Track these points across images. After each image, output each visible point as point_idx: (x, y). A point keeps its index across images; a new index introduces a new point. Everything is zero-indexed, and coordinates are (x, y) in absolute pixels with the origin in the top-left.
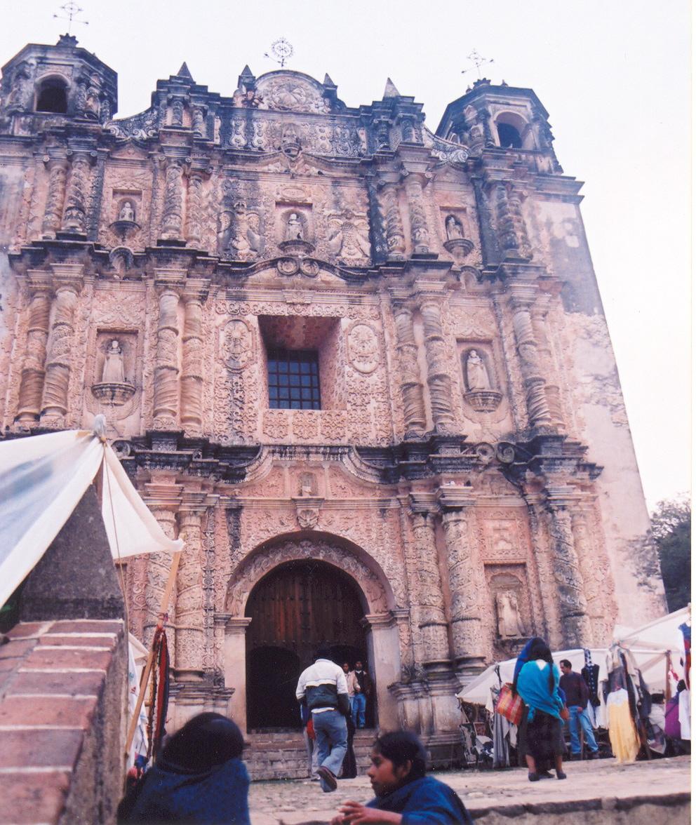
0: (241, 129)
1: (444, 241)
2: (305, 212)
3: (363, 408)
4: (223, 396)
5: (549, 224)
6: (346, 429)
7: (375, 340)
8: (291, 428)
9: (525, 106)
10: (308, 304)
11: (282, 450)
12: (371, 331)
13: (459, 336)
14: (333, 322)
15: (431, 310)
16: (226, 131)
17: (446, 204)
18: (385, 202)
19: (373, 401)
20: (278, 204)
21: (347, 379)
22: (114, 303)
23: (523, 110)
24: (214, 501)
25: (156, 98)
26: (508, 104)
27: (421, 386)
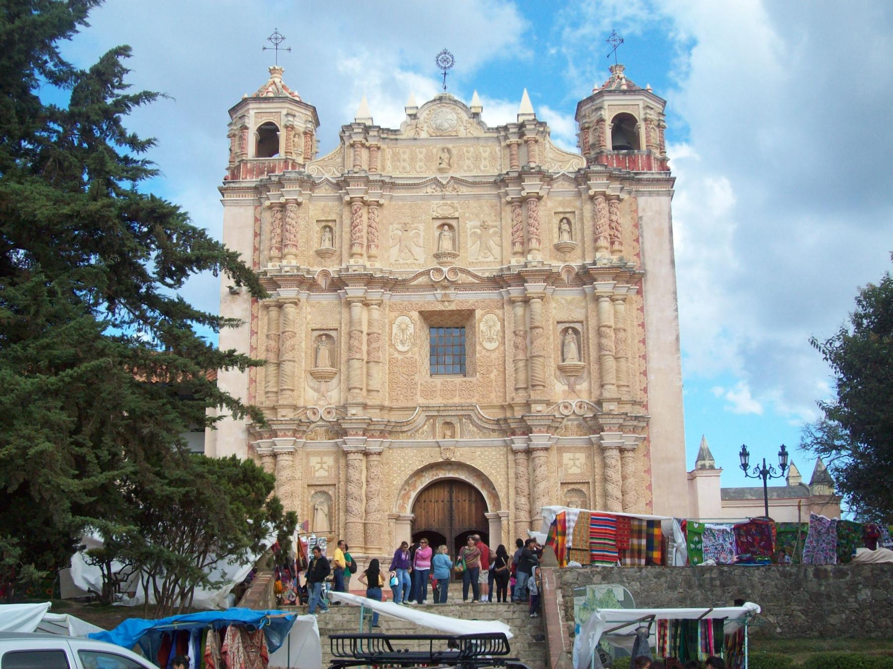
1: (556, 241)
7: (498, 327)
8: (438, 392)
13: (560, 320)
14: (470, 313)
15: (537, 305)
17: (561, 210)
21: (478, 355)
23: (635, 106)
25: (342, 138)
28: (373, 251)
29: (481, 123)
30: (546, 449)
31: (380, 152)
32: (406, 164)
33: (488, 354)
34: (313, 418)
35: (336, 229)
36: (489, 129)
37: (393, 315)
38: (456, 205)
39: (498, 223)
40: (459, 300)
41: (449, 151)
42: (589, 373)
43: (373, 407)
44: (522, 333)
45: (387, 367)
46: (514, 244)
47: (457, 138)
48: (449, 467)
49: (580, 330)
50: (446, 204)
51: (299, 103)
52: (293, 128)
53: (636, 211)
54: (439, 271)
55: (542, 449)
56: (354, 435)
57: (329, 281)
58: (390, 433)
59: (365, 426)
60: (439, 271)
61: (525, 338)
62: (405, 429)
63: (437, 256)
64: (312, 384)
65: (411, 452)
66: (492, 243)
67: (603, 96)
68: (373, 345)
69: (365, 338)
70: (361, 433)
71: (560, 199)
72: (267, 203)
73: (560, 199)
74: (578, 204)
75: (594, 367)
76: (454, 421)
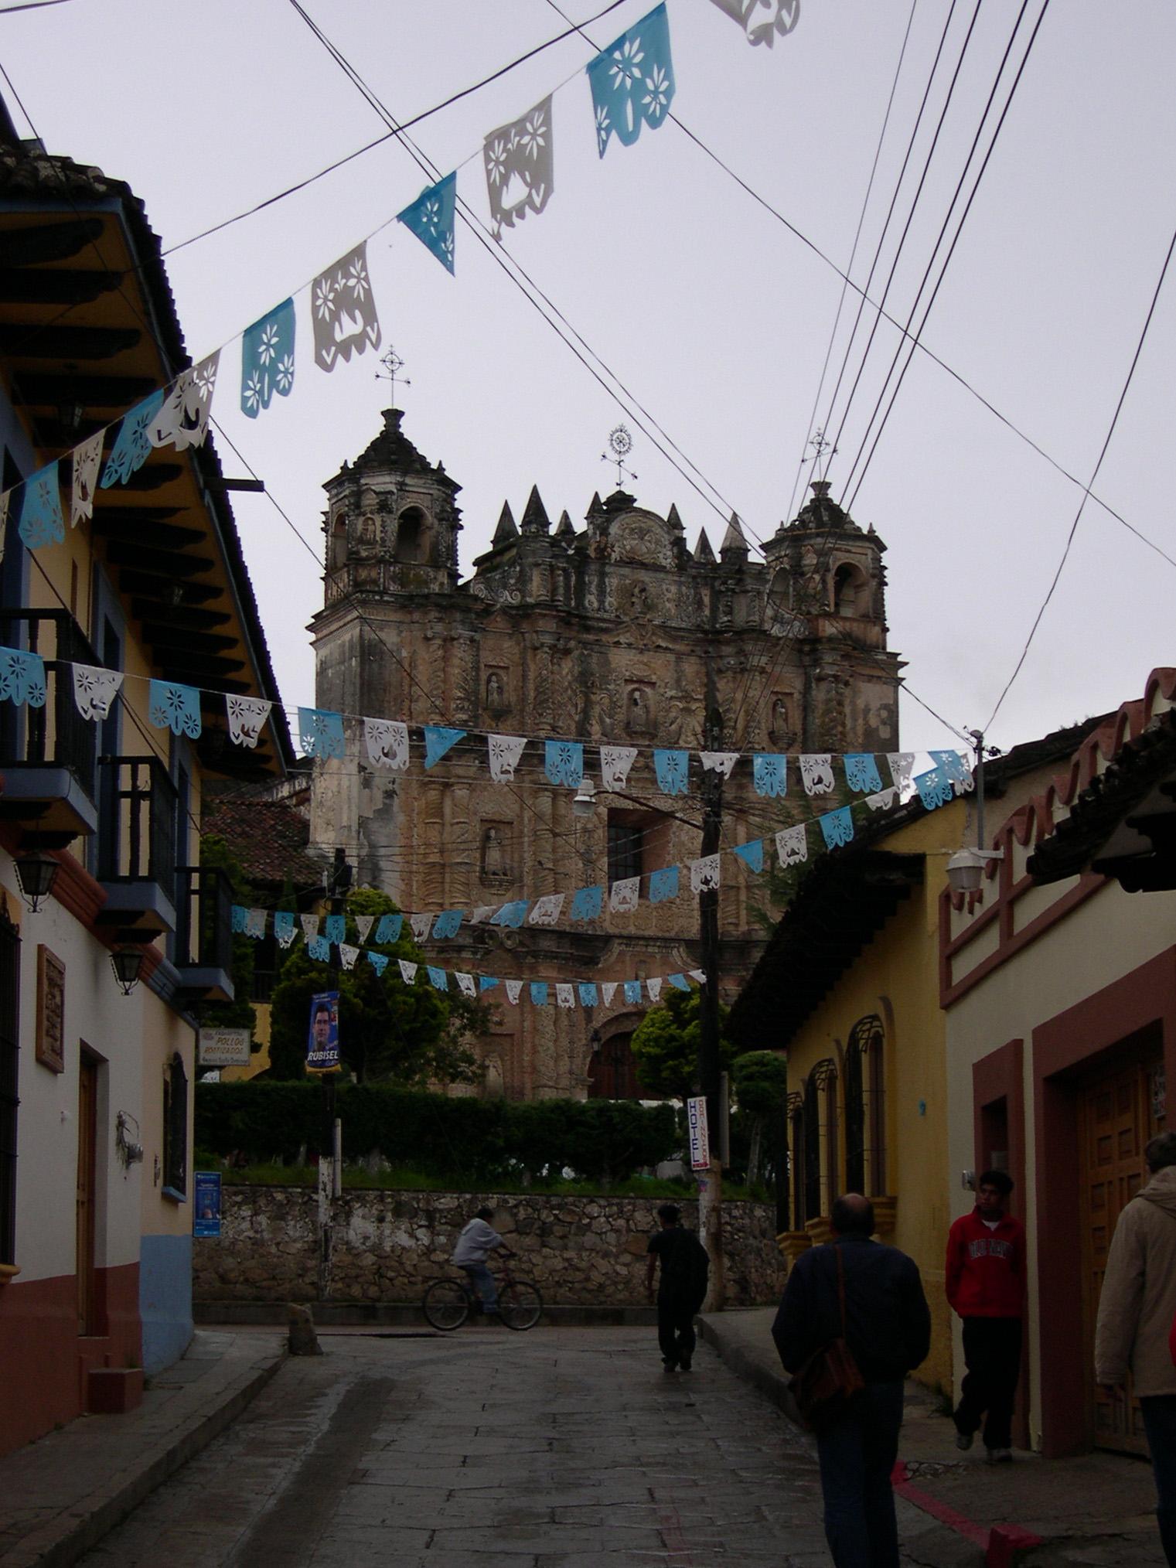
0: (593, 589)
5: (867, 710)
11: (629, 939)
16: (581, 590)
18: (722, 684)
26: (849, 551)
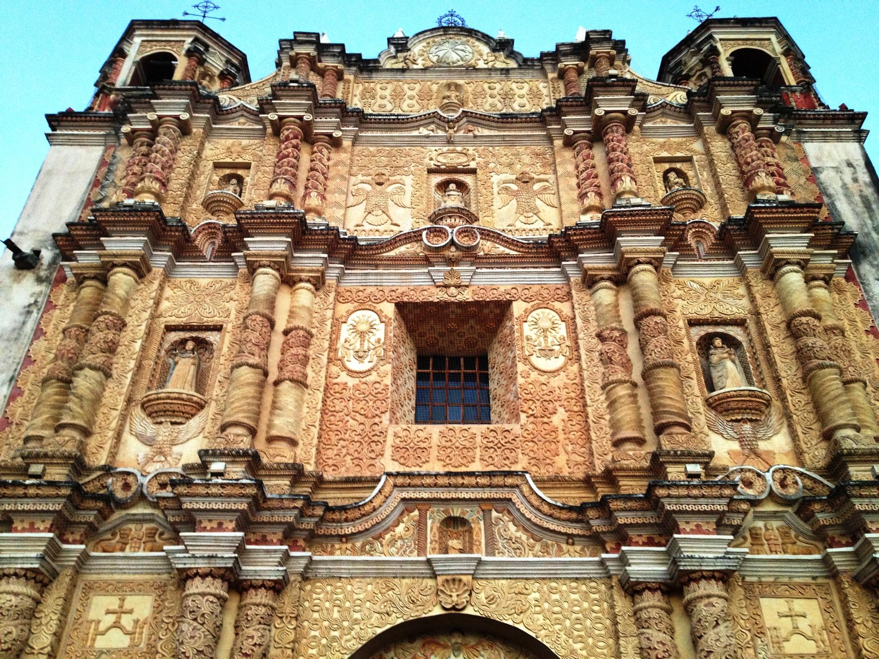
1: (661, 197)
2: (468, 179)
3: (545, 420)
4: (337, 408)
6: (519, 451)
7: (562, 330)
8: (434, 452)
9: (769, 39)
10: (467, 286)
12: (557, 317)
14: (502, 308)
15: (644, 277)
17: (665, 154)
19: (561, 410)
20: (430, 171)
21: (520, 380)
22: (201, 291)
24: (304, 562)
27: (635, 385)
28: (314, 201)
29: (512, 55)
30: (724, 577)
31: (341, 85)
32: (385, 102)
33: (543, 379)
34: (120, 494)
35: (248, 180)
36: (526, 60)
37: (342, 309)
38: (470, 152)
39: (551, 177)
40: (480, 284)
41: (458, 87)
42: (787, 416)
43: (276, 471)
44: (617, 334)
45: (320, 396)
46: (582, 196)
47: (471, 69)
48: (457, 639)
49: (739, 338)
50: (453, 152)
51: (216, 36)
52: (202, 62)
53: (805, 158)
54: (439, 232)
55: (711, 576)
56: (212, 530)
57: (218, 242)
58: (313, 539)
59: (244, 506)
60: (440, 232)
61: (623, 345)
62: (348, 529)
63: (437, 217)
64: (139, 428)
65: (361, 590)
66: (538, 203)
67: (709, 29)
68: (294, 351)
69: (278, 340)
70: (232, 525)
71: (662, 140)
72: (126, 129)
73: (662, 140)
74: (697, 146)
75: (798, 401)
76: (471, 514)
